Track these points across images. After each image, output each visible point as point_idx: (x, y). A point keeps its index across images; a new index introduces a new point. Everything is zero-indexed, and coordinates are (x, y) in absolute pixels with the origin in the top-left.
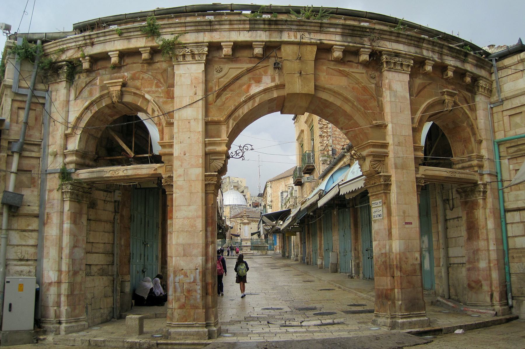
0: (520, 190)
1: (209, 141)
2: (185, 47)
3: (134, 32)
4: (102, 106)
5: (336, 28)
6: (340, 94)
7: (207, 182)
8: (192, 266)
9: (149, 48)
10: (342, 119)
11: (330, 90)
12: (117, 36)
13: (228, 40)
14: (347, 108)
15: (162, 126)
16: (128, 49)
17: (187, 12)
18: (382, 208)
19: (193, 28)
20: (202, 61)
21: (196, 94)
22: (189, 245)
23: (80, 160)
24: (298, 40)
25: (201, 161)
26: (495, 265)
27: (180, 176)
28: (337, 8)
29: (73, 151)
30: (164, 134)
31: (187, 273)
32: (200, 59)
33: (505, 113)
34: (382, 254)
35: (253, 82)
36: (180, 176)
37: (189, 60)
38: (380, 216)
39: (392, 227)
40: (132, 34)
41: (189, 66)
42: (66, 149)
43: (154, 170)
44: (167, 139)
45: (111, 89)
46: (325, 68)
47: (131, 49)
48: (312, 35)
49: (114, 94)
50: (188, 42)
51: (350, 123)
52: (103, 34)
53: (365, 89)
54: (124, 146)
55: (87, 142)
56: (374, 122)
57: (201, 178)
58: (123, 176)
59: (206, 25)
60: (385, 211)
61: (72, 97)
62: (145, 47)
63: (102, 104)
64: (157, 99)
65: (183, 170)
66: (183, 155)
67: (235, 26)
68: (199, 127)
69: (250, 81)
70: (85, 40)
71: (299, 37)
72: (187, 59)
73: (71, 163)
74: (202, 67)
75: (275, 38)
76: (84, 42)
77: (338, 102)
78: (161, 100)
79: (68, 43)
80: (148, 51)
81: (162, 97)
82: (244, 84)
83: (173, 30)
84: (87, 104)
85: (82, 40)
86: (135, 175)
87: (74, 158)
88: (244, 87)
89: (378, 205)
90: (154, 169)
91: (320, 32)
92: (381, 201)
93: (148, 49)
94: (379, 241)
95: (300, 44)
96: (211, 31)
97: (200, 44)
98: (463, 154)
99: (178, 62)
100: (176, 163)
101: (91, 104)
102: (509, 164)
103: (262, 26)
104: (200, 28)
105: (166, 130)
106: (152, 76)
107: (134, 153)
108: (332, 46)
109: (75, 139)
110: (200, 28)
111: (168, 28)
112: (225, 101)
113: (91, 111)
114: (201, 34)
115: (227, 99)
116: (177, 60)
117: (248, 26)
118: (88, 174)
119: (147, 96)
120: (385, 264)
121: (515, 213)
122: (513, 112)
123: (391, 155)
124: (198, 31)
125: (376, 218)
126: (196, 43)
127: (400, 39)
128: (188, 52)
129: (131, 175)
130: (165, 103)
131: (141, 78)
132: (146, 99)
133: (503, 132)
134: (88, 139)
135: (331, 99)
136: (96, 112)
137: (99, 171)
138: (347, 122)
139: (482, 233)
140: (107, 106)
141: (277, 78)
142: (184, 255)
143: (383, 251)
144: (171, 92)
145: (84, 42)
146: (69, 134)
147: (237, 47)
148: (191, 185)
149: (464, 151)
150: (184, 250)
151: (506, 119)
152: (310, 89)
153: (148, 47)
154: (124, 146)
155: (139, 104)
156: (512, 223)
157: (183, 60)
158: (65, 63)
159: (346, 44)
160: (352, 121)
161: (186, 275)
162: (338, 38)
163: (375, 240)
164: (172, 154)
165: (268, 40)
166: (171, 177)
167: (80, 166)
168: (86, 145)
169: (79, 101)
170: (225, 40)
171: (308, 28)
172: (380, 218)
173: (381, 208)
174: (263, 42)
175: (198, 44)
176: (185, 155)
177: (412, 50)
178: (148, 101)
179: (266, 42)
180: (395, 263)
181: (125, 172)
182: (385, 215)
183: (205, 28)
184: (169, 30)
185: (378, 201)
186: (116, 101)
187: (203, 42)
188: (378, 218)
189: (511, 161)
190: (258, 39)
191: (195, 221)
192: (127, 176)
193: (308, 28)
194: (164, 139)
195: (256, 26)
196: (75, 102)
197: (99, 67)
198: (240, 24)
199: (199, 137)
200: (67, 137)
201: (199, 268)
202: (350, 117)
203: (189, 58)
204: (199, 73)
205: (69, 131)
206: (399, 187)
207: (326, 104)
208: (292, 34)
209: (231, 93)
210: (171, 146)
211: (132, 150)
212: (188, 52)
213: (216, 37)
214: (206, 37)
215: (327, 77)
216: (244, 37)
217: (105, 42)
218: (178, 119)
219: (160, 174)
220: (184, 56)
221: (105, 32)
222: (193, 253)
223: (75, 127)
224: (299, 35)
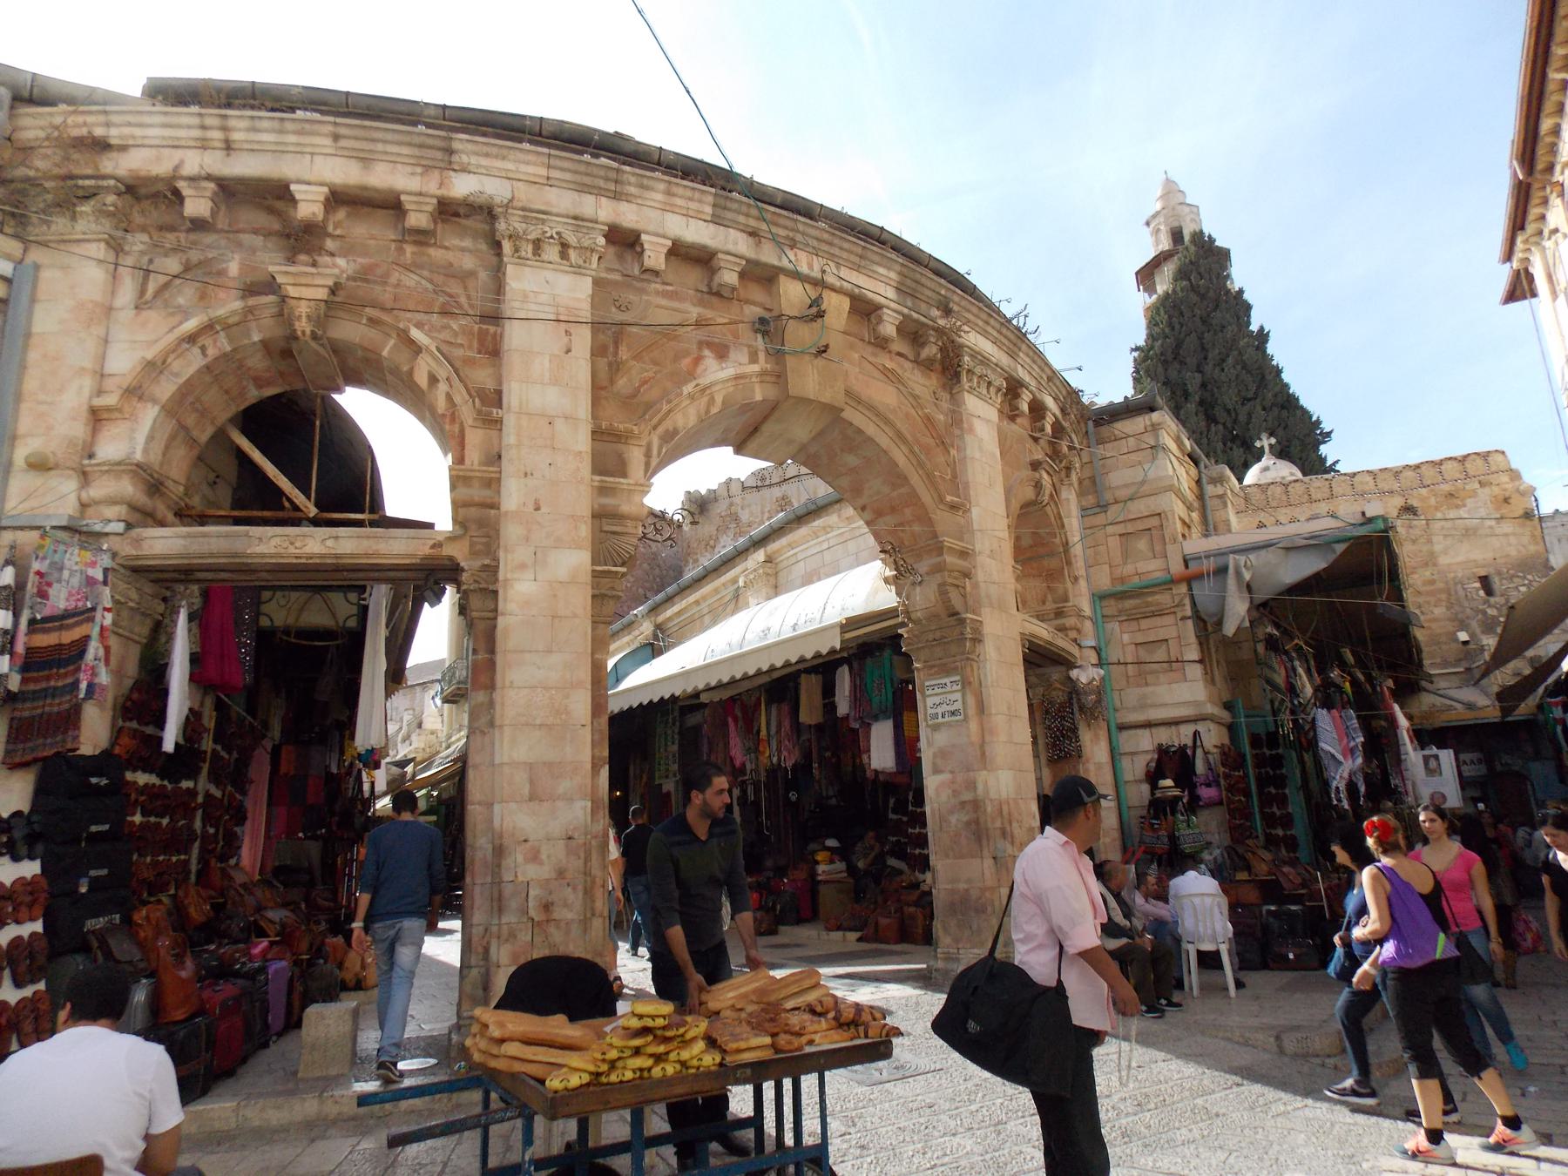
0: (1147, 684)
1: (602, 481)
2: (543, 222)
3: (385, 142)
4: (246, 341)
5: (889, 269)
6: (887, 422)
7: (597, 592)
8: (557, 827)
9: (435, 201)
10: (876, 486)
11: (871, 408)
12: (328, 142)
13: (661, 231)
14: (900, 456)
15: (462, 424)
16: (365, 188)
17: (540, 135)
19: (568, 176)
20: (588, 272)
21: (568, 351)
22: (549, 765)
23: (142, 499)
24: (816, 274)
25: (585, 531)
26: (1114, 840)
28: (882, 229)
29: (119, 463)
30: (468, 447)
31: (538, 851)
32: (581, 262)
33: (1110, 529)
34: (963, 803)
35: (707, 352)
37: (551, 259)
38: (953, 713)
39: (987, 738)
40: (380, 147)
41: (549, 275)
42: (91, 456)
43: (433, 547)
44: (476, 462)
45: (292, 291)
46: (856, 356)
47: (376, 190)
48: (844, 273)
49: (303, 309)
50: (555, 210)
51: (895, 494)
52: (276, 124)
53: (929, 421)
54: (284, 483)
55: (167, 447)
56: (949, 498)
58: (322, 556)
59: (607, 179)
61: (127, 292)
62: (420, 194)
63: (248, 334)
64: (445, 348)
65: (532, 549)
66: (531, 508)
67: (679, 202)
68: (582, 441)
69: (700, 349)
70: (203, 127)
71: (816, 267)
72: (545, 257)
73: (112, 502)
74: (587, 284)
75: (769, 255)
76: (197, 133)
77: (884, 441)
78: (459, 352)
79: (129, 124)
80: (430, 208)
81: (462, 345)
82: (687, 353)
83: (510, 166)
84: (191, 325)
85: (189, 127)
86: (367, 555)
87: (127, 488)
88: (686, 363)
89: (948, 689)
90: (432, 542)
91: (858, 268)
93: (428, 200)
94: (952, 772)
95: (819, 283)
96: (617, 196)
97: (585, 224)
98: (1044, 603)
99: (519, 258)
100: (511, 532)
101: (209, 328)
102: (1122, 632)
103: (741, 219)
104: (587, 180)
105: (475, 438)
106: (431, 281)
107: (316, 505)
108: (879, 307)
109: (133, 430)
110: (587, 180)
111: (496, 157)
112: (640, 386)
113: (203, 349)
114: (589, 200)
115: (646, 382)
116: (517, 250)
117: (708, 210)
118: (181, 542)
119: (415, 334)
120: (973, 826)
121: (1140, 732)
122: (1130, 528)
123: (980, 576)
124: (583, 189)
125: (940, 720)
126: (575, 218)
127: (989, 329)
128: (552, 237)
129: (352, 556)
130: (469, 362)
131: (393, 280)
132: (411, 342)
133: (1106, 567)
134: (172, 438)
135: (871, 429)
136: (225, 356)
137: (227, 536)
138: (886, 490)
140: (265, 344)
141: (762, 356)
142: (533, 797)
143: (967, 796)
144: (489, 338)
145: (197, 133)
146: (109, 409)
147: (680, 252)
148: (555, 596)
149: (1045, 596)
150: (531, 782)
151: (1114, 542)
152: (832, 395)
153: (432, 196)
154: (284, 483)
155: (385, 353)
156: (1133, 754)
157: (534, 255)
158: (112, 182)
159: (906, 311)
160: (903, 490)
161: (534, 857)
162: (891, 293)
163: (936, 771)
164: (495, 506)
165: (751, 254)
166: (492, 570)
167: (142, 516)
168: (164, 455)
169: (152, 316)
170: (651, 228)
171: (836, 251)
173: (958, 696)
174: (741, 257)
175: (580, 223)
176: (537, 509)
177: (1004, 360)
178: (416, 349)
179: (748, 261)
180: (998, 824)
181: (330, 543)
182: (972, 711)
183: (602, 183)
184: (499, 164)
186: (308, 332)
187: (596, 222)
188: (947, 719)
189: (1125, 624)
190: (730, 247)
191: (567, 697)
192: (337, 556)
193: (836, 251)
194: (467, 461)
195: (729, 215)
196: (137, 315)
197: (241, 226)
198: (691, 199)
199: (578, 469)
200: (97, 417)
201: (576, 836)
202: (897, 478)
203: (552, 252)
204: (578, 300)
205: (110, 400)
206: (998, 649)
207: (854, 440)
208: (803, 256)
209: (656, 368)
210: (493, 483)
211: (306, 491)
212: (552, 237)
213: (628, 215)
214: (606, 211)
215: (860, 376)
216: (698, 233)
217: (279, 151)
218: (517, 410)
219: (451, 558)
220: (537, 245)
221: (282, 119)
222: (561, 790)
223: (135, 393)
224: (817, 263)
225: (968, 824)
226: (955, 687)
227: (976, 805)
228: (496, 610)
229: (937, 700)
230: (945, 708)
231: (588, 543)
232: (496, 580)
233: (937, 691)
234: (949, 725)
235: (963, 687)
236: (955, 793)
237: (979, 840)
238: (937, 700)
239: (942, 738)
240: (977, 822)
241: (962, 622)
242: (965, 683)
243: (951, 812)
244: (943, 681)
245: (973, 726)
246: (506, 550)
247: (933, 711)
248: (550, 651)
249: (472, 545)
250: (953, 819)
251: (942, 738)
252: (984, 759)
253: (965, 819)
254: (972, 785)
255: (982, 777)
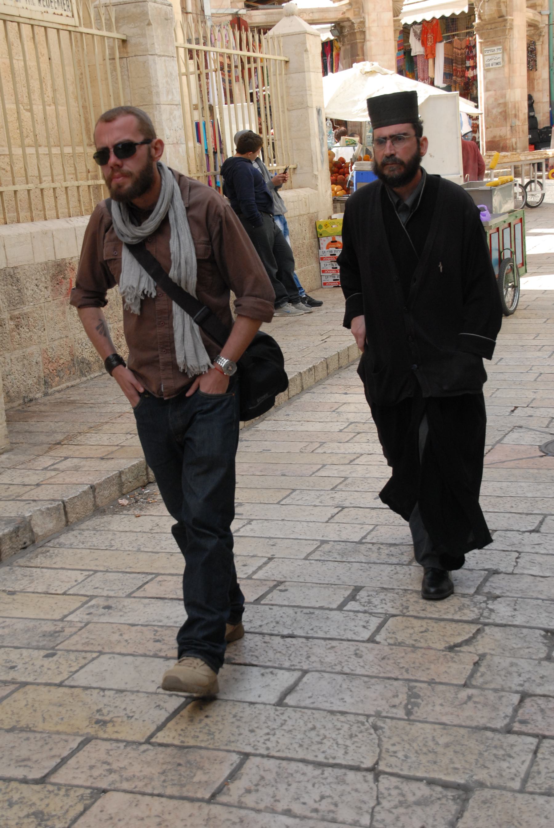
18: (503, 56)
27: (374, 21)
34: (499, 104)
36: (374, 21)
38: (497, 64)
57: (392, 23)
60: (506, 58)
89: (496, 52)
92: (501, 47)
120: (503, 114)
125: (491, 67)
139: (538, 83)
143: (501, 101)
166: (363, 23)
172: (498, 66)
173: (500, 56)
180: (513, 112)
181: (311, 15)
185: (495, 48)
188: (494, 66)
225: (501, 113)
226: (499, 52)
227: (505, 104)
228: (364, 39)
229: (490, 57)
230: (493, 61)
231: (392, 9)
232: (365, 27)
233: (490, 53)
234: (495, 69)
235: (503, 52)
236: (496, 99)
237: (505, 119)
238: (490, 57)
239: (491, 75)
240: (505, 112)
241: (506, 20)
242: (504, 50)
243: (493, 108)
244: (493, 48)
245: (506, 69)
246: (368, 15)
247: (487, 63)
248: (384, 54)
249: (354, 11)
250: (494, 111)
251: (491, 75)
252: (510, 85)
253: (500, 110)
254: (504, 96)
255: (509, 92)
